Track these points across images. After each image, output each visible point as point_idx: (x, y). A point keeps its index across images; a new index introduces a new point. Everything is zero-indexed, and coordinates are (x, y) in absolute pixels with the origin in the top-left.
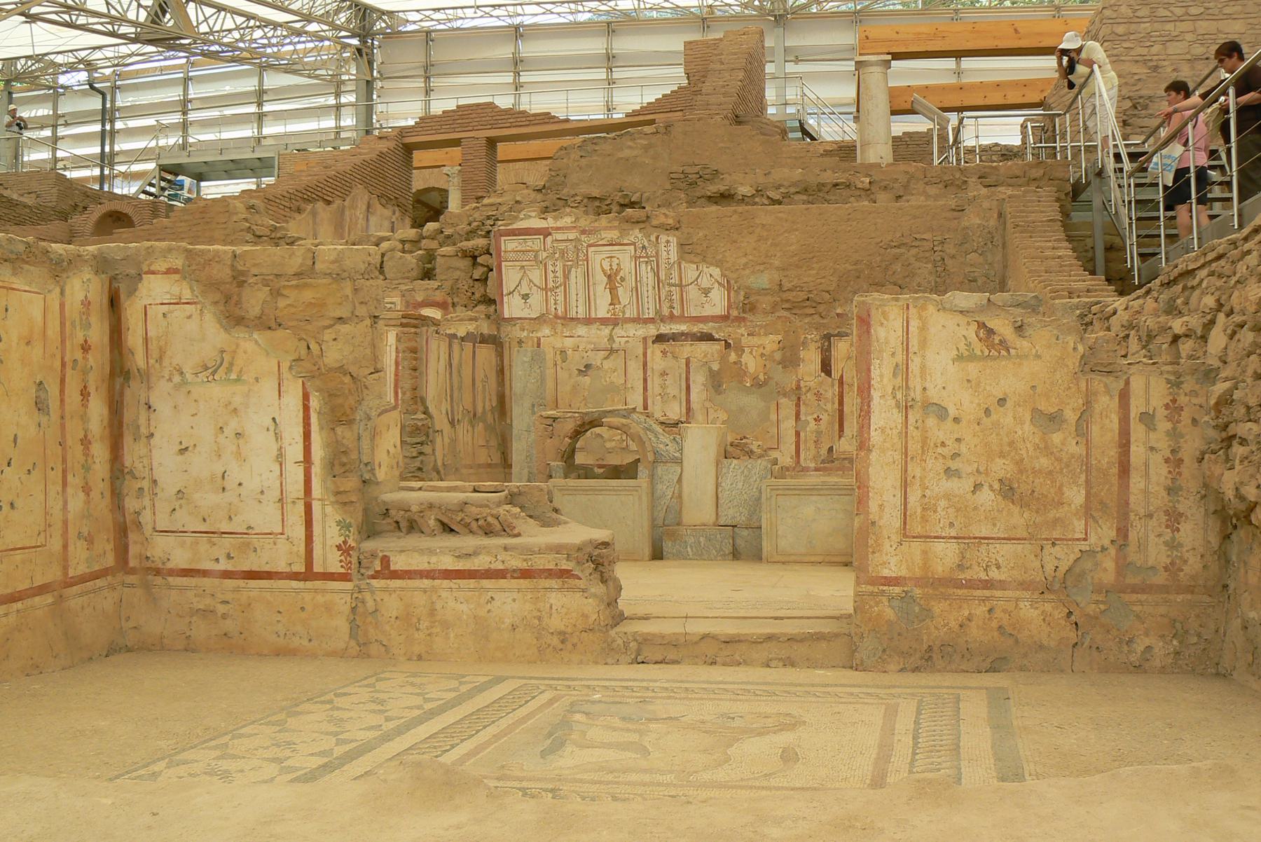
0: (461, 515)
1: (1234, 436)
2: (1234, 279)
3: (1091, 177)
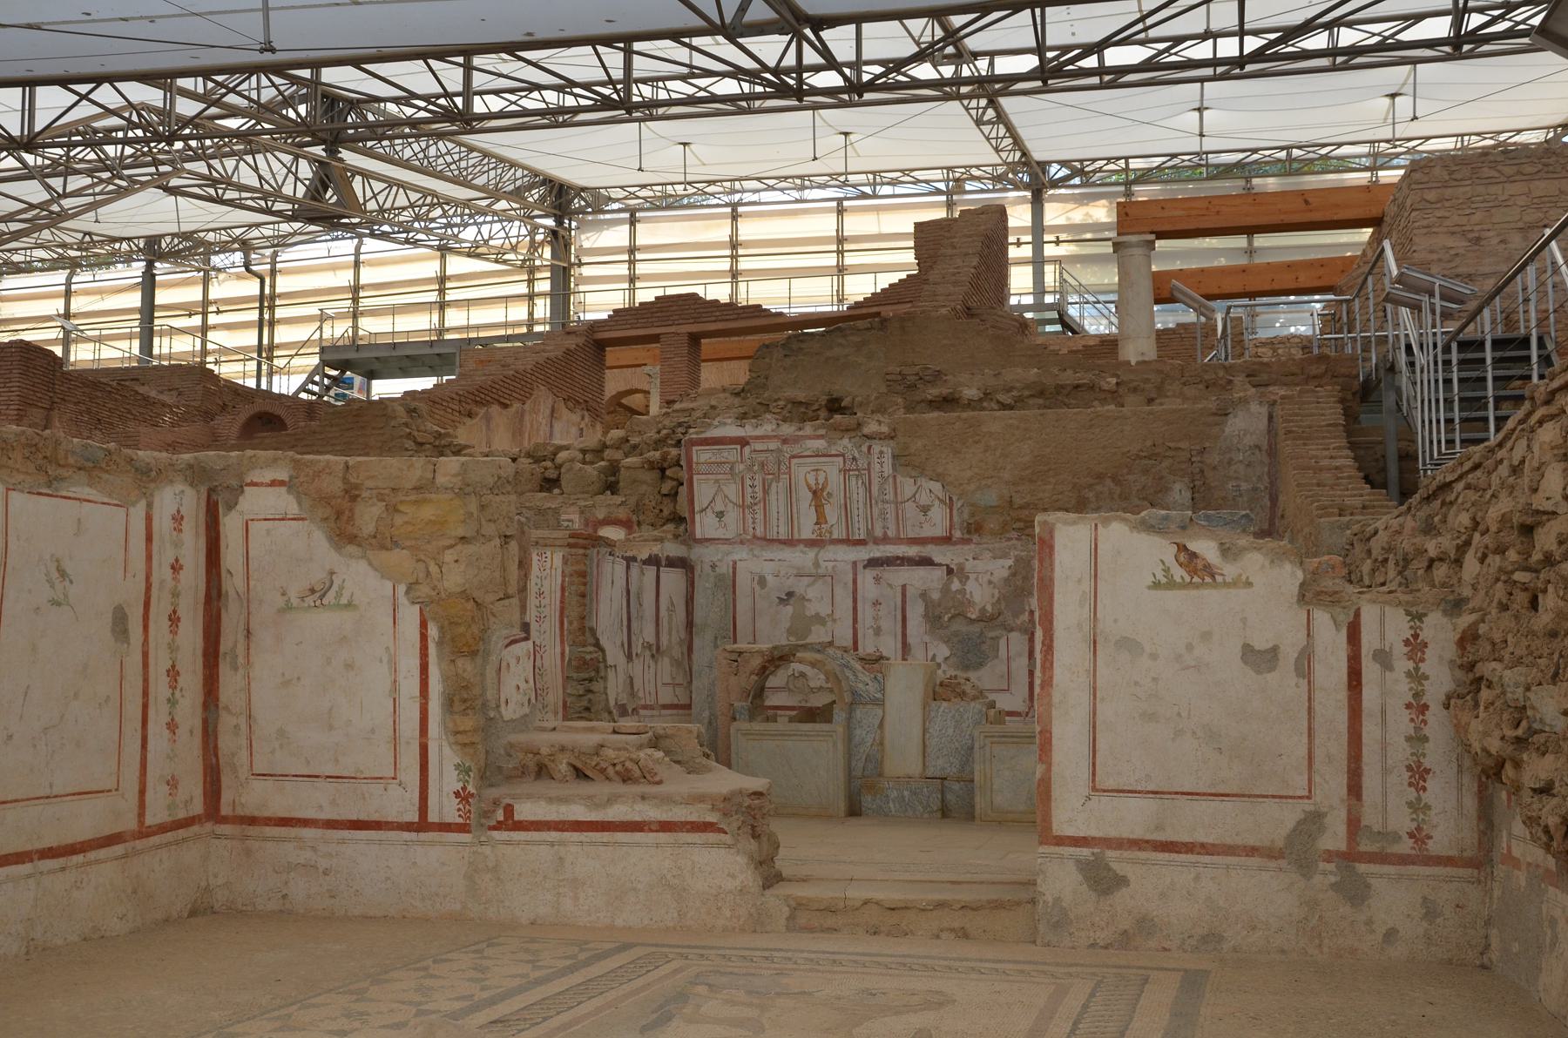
0: (596, 759)
1: (1481, 678)
2: (1490, 492)
3: (1382, 372)
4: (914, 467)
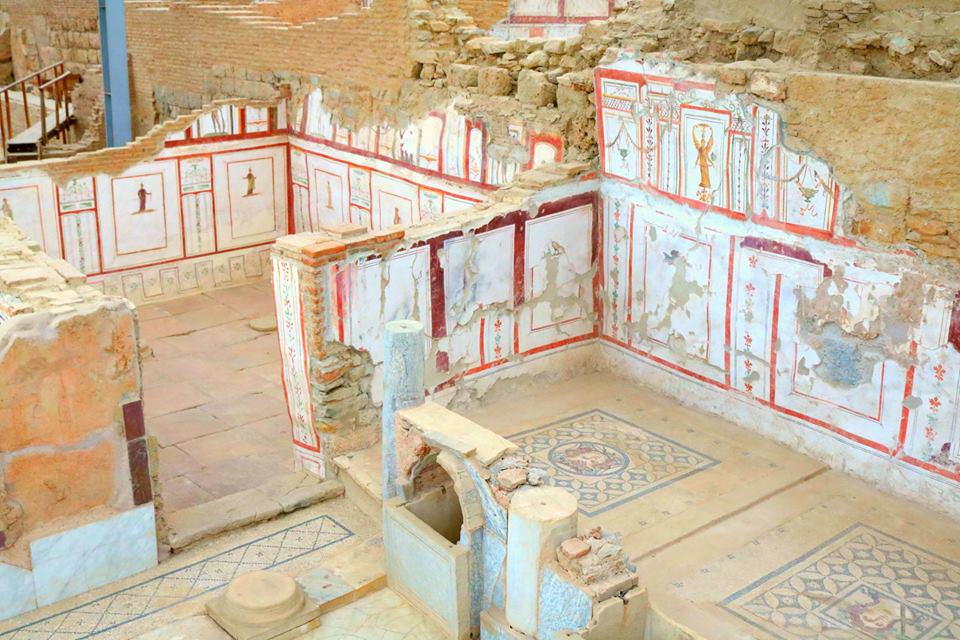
4: (804, 140)
